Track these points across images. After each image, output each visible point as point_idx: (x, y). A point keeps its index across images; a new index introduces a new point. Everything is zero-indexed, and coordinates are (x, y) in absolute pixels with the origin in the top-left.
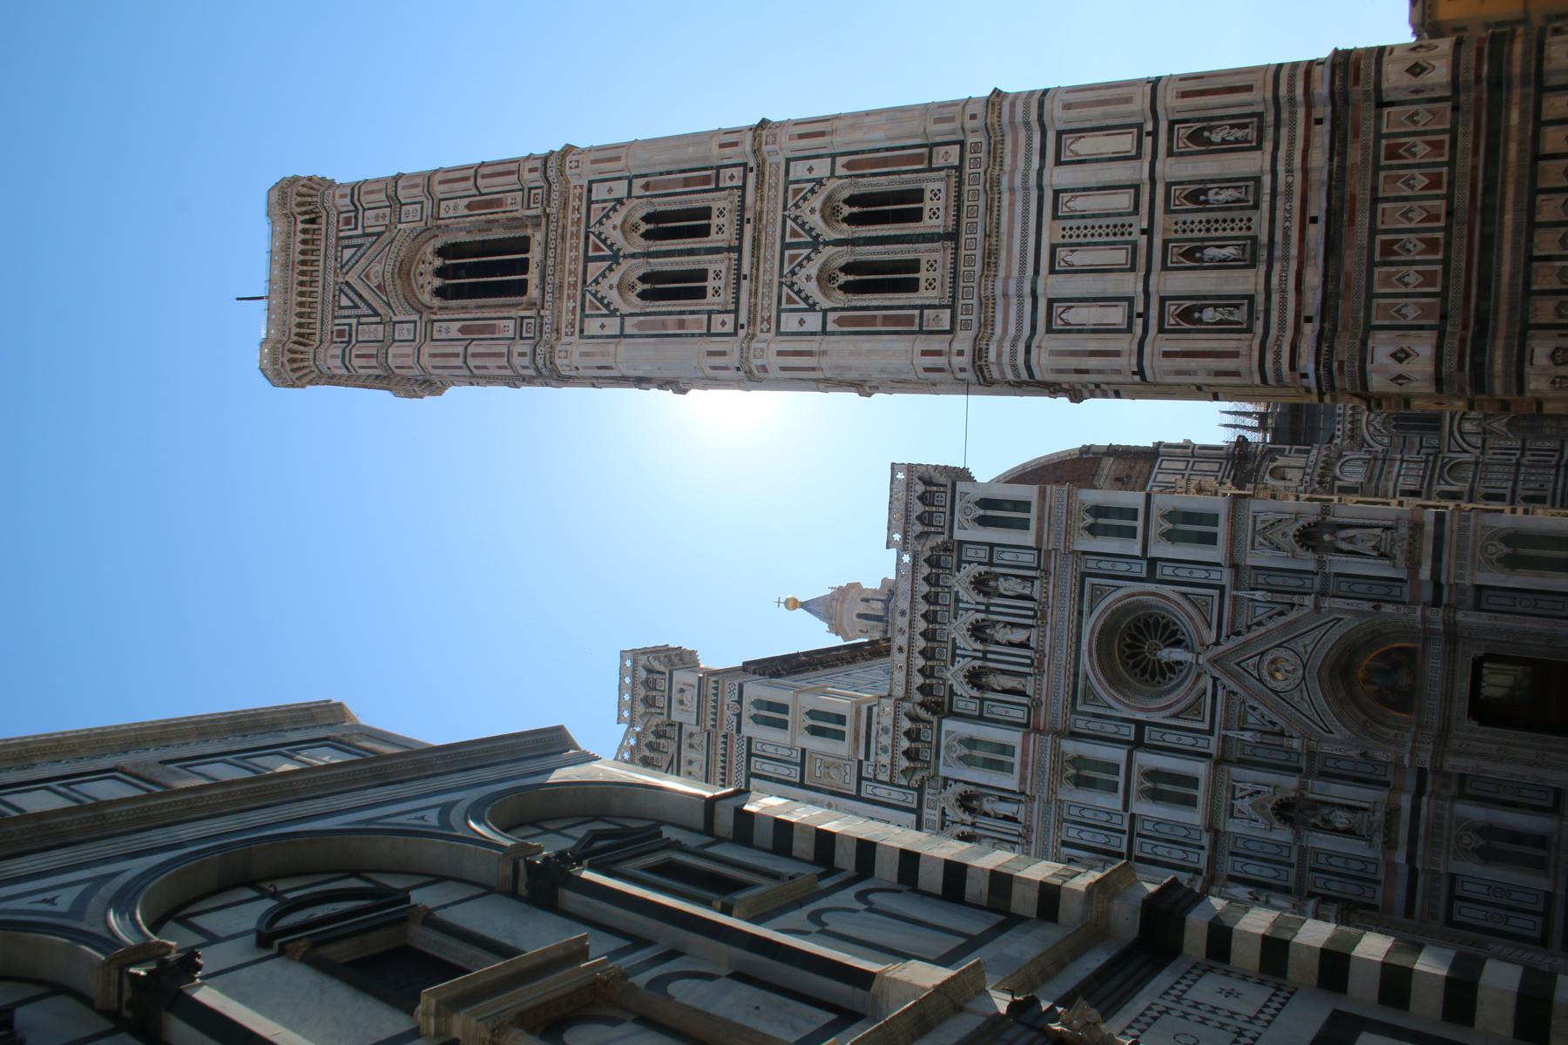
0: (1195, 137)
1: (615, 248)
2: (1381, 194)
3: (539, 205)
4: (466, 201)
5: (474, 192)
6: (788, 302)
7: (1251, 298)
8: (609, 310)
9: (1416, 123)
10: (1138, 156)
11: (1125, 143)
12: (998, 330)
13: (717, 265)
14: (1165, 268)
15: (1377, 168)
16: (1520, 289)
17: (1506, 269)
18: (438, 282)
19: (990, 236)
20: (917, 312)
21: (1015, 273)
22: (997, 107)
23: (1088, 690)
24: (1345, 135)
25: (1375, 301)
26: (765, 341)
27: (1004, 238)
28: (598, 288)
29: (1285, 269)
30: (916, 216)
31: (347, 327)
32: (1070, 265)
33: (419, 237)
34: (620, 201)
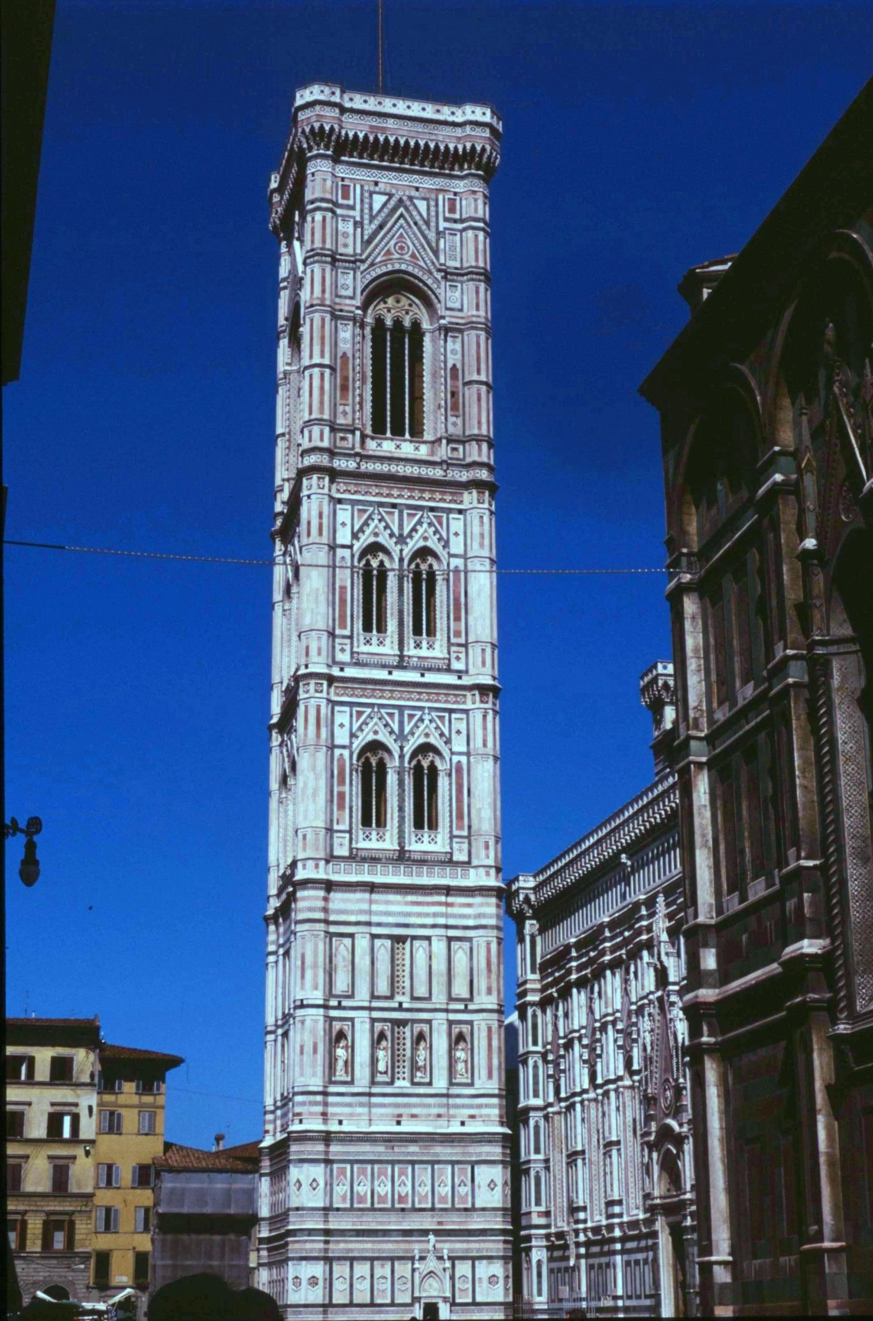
1: (408, 540)
3: (450, 455)
4: (459, 366)
5: (466, 380)
6: (358, 712)
7: (352, 1083)
8: (358, 531)
10: (451, 999)
11: (460, 989)
13: (389, 648)
14: (373, 1020)
18: (389, 322)
21: (374, 907)
25: (348, 1167)
26: (328, 693)
28: (376, 521)
30: (418, 825)
31: (351, 202)
33: (429, 304)
34: (446, 545)
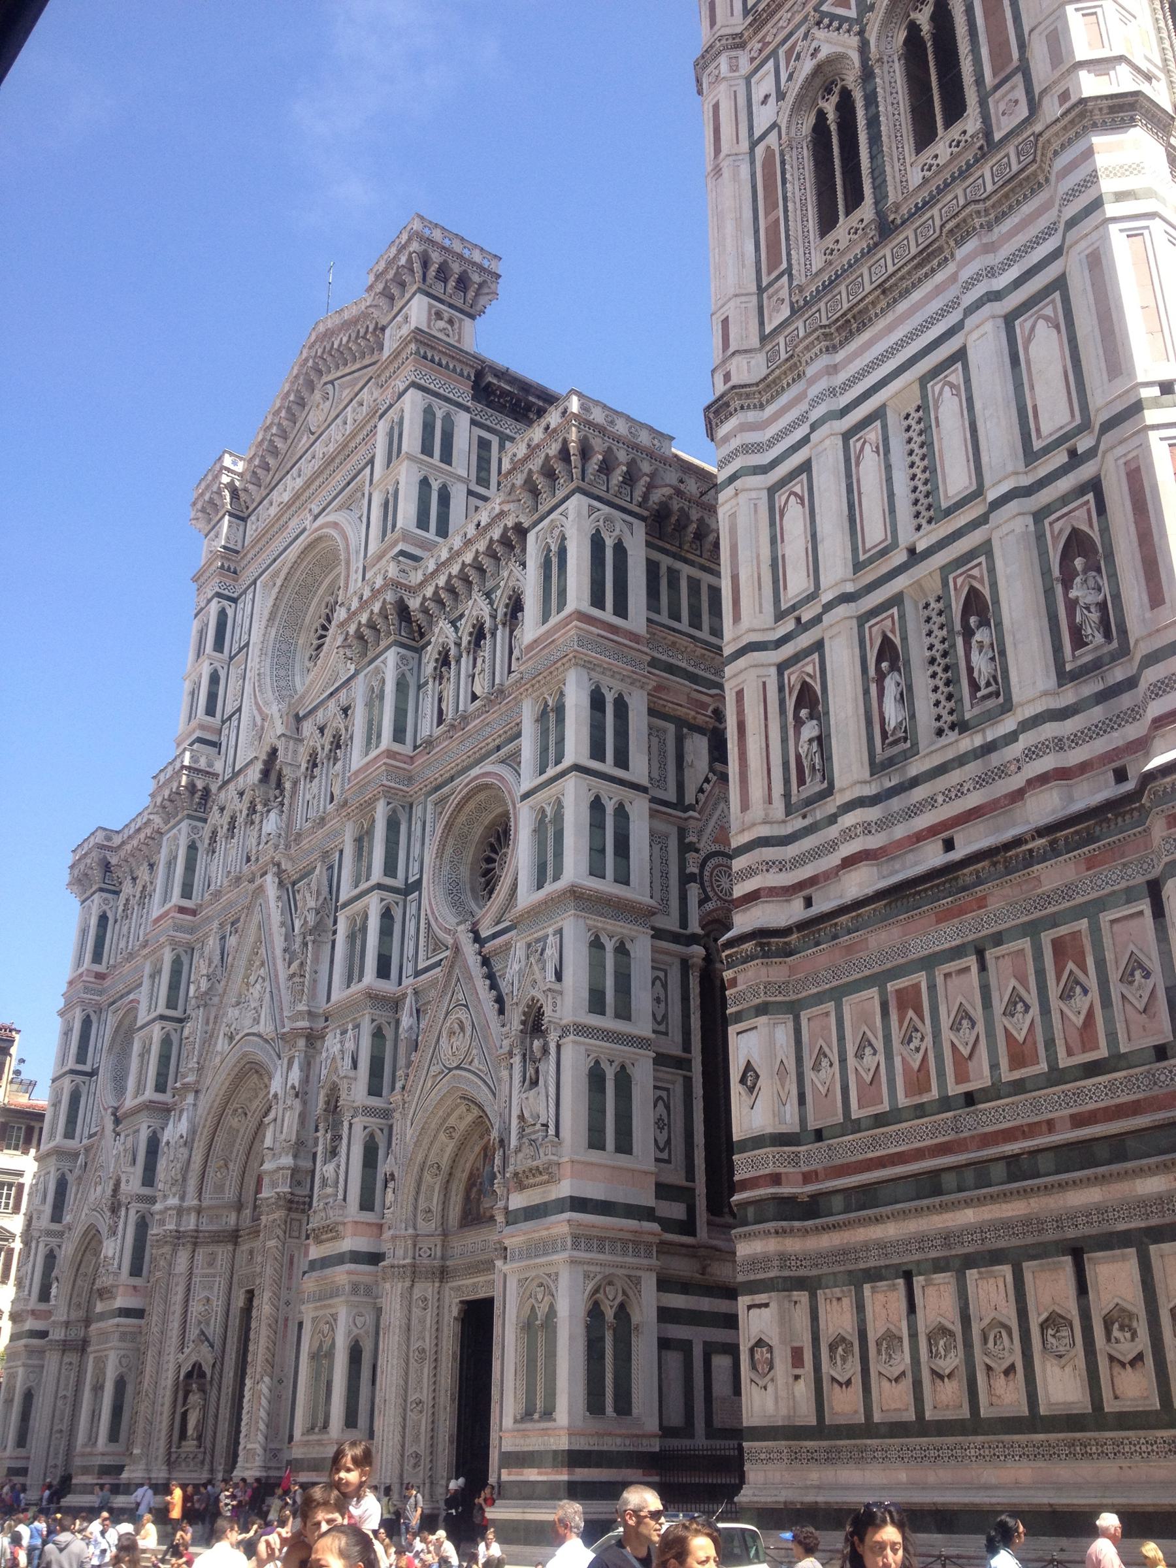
0: (1077, 543)
2: (990, 955)
9: (1127, 978)
12: (770, 410)
15: (1032, 929)
16: (862, 1266)
17: (890, 1231)
19: (884, 292)
20: (784, 265)
21: (842, 376)
22: (1078, 128)
23: (443, 801)
24: (1091, 839)
27: (890, 317)
29: (867, 828)
32: (858, 458)
